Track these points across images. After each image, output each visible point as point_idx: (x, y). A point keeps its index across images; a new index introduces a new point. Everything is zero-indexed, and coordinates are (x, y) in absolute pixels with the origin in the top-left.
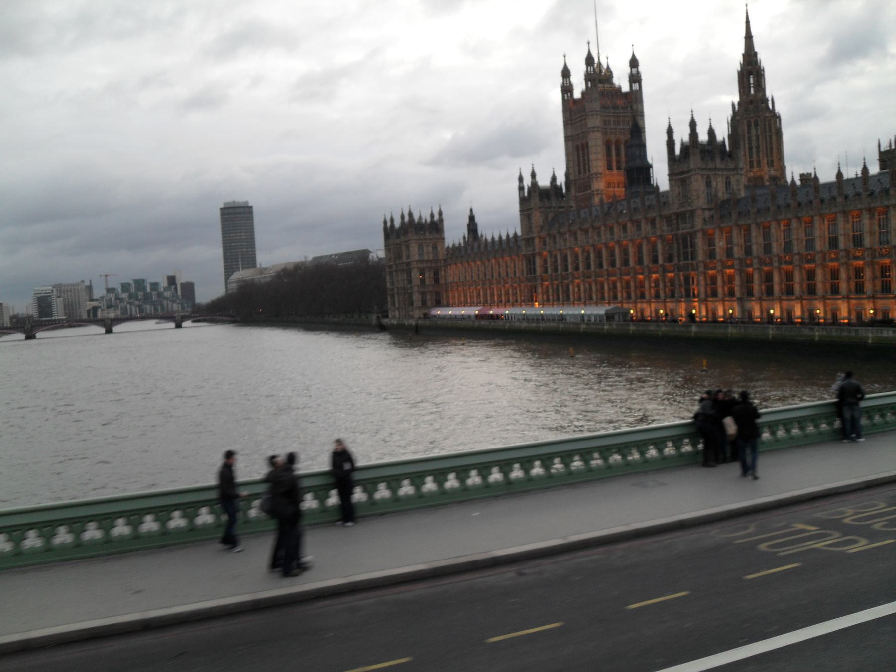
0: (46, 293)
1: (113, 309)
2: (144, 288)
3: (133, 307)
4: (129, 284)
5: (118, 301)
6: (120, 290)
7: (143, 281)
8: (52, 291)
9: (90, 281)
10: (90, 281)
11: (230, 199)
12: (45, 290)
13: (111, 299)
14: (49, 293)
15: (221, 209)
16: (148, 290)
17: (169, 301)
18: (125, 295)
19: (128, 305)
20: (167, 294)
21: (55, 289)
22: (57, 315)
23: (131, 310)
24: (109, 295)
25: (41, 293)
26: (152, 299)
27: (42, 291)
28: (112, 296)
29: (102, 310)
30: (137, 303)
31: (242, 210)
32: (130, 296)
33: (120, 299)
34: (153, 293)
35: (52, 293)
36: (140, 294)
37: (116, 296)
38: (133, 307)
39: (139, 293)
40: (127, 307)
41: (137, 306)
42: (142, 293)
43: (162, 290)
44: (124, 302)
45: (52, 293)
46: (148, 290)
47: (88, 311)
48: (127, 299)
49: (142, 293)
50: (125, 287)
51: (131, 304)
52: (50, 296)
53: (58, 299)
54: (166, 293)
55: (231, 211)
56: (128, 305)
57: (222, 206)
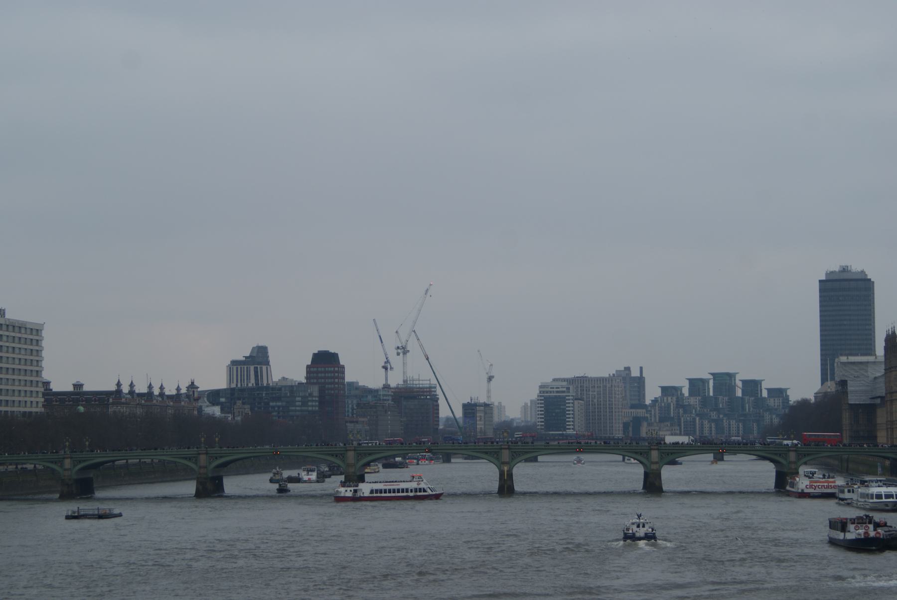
0: (557, 392)
1: (669, 424)
2: (732, 389)
3: (706, 422)
4: (704, 382)
5: (681, 411)
6: (686, 392)
7: (731, 376)
8: (568, 388)
9: (641, 368)
10: (641, 368)
12: (557, 388)
13: (669, 405)
14: (563, 392)
15: (820, 281)
16: (739, 393)
17: (774, 416)
18: (694, 401)
19: (697, 419)
20: (772, 402)
21: (571, 387)
22: (573, 429)
23: (702, 425)
24: (665, 398)
25: (551, 392)
26: (743, 408)
27: (551, 388)
28: (671, 400)
29: (649, 425)
30: (714, 415)
32: (705, 401)
33: (683, 406)
34: (747, 398)
35: (569, 392)
36: (723, 401)
37: (677, 401)
38: (706, 422)
39: (720, 398)
40: (694, 419)
41: (714, 421)
42: (726, 398)
43: (765, 394)
44: (691, 413)
45: (569, 392)
46: (739, 393)
47: (626, 426)
48: (698, 409)
49: (726, 398)
50: (696, 385)
51: (701, 416)
53: (576, 402)
54: (772, 400)
56: (697, 419)
57: (824, 278)
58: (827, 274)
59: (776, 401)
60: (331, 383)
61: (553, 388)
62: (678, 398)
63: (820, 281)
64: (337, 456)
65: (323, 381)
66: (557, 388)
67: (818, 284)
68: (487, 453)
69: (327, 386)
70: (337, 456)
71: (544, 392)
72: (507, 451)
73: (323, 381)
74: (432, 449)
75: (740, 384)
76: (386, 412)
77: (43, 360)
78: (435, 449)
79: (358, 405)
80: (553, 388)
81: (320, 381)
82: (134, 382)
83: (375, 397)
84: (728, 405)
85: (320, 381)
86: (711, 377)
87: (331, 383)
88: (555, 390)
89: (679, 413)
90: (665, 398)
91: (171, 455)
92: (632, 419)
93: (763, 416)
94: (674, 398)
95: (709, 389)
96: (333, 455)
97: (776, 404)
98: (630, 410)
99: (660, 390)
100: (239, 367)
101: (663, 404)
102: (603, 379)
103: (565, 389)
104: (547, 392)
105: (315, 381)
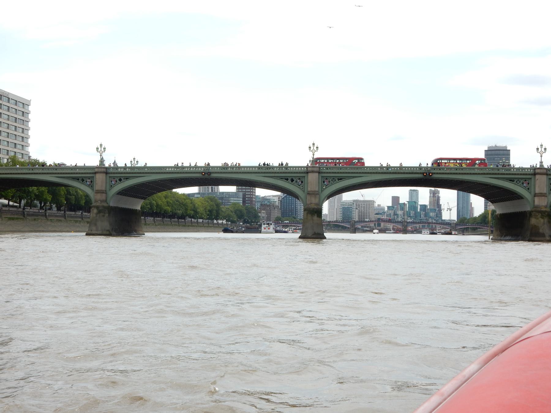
0: (348, 205)
8: (353, 204)
11: (492, 144)
12: (348, 203)
14: (351, 205)
15: (485, 151)
17: (433, 220)
24: (389, 211)
25: (345, 205)
26: (421, 217)
28: (392, 212)
31: (501, 152)
33: (396, 215)
48: (402, 216)
52: (351, 207)
55: (493, 152)
57: (487, 149)
58: (488, 147)
59: (433, 214)
60: (249, 192)
61: (347, 203)
62: (394, 211)
63: (485, 151)
64: (292, 180)
65: (245, 190)
66: (348, 203)
67: (484, 151)
68: (513, 181)
69: (247, 193)
70: (292, 180)
71: (342, 205)
72: (545, 177)
73: (245, 190)
74: (432, 173)
75: (419, 206)
76: (275, 209)
77: (30, 130)
78: (437, 173)
79: (261, 205)
80: (347, 203)
81: (243, 190)
82: (116, 161)
83: (269, 202)
84: (415, 215)
85: (243, 190)
86: (407, 203)
87: (249, 192)
88: (347, 204)
89: (395, 218)
90: (389, 211)
91: (56, 173)
92: (377, 219)
93: (429, 220)
94: (393, 211)
95: (407, 207)
96: (287, 180)
97: (433, 215)
98: (375, 215)
99: (387, 207)
100: (204, 187)
101: (388, 214)
102: (363, 201)
103: (352, 204)
104: (344, 205)
105: (241, 190)
